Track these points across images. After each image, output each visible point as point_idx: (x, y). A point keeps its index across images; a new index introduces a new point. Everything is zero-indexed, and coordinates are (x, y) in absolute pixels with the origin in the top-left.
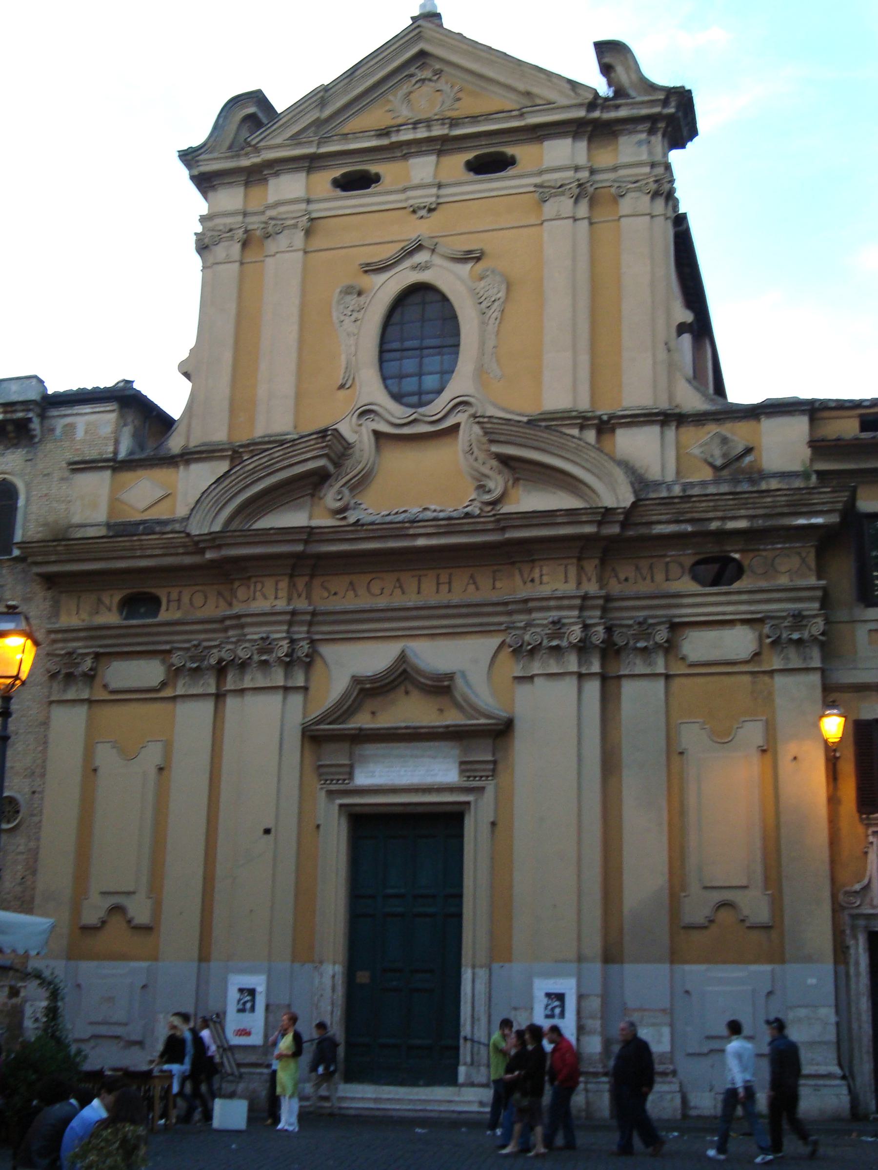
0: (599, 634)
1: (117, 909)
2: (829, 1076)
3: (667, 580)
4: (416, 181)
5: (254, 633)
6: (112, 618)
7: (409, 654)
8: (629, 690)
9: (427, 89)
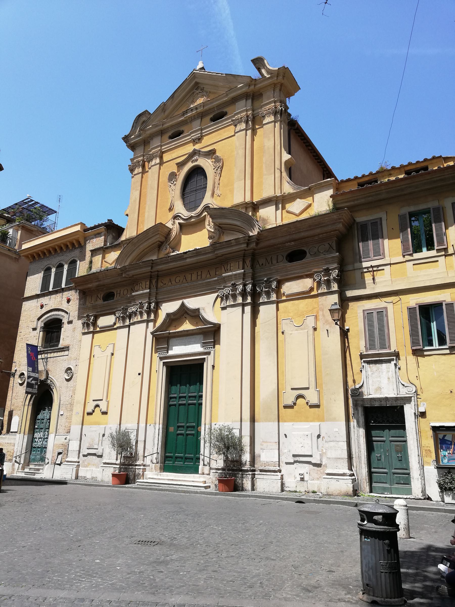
0: (249, 288)
1: (97, 406)
2: (344, 475)
6: (100, 302)
8: (262, 308)
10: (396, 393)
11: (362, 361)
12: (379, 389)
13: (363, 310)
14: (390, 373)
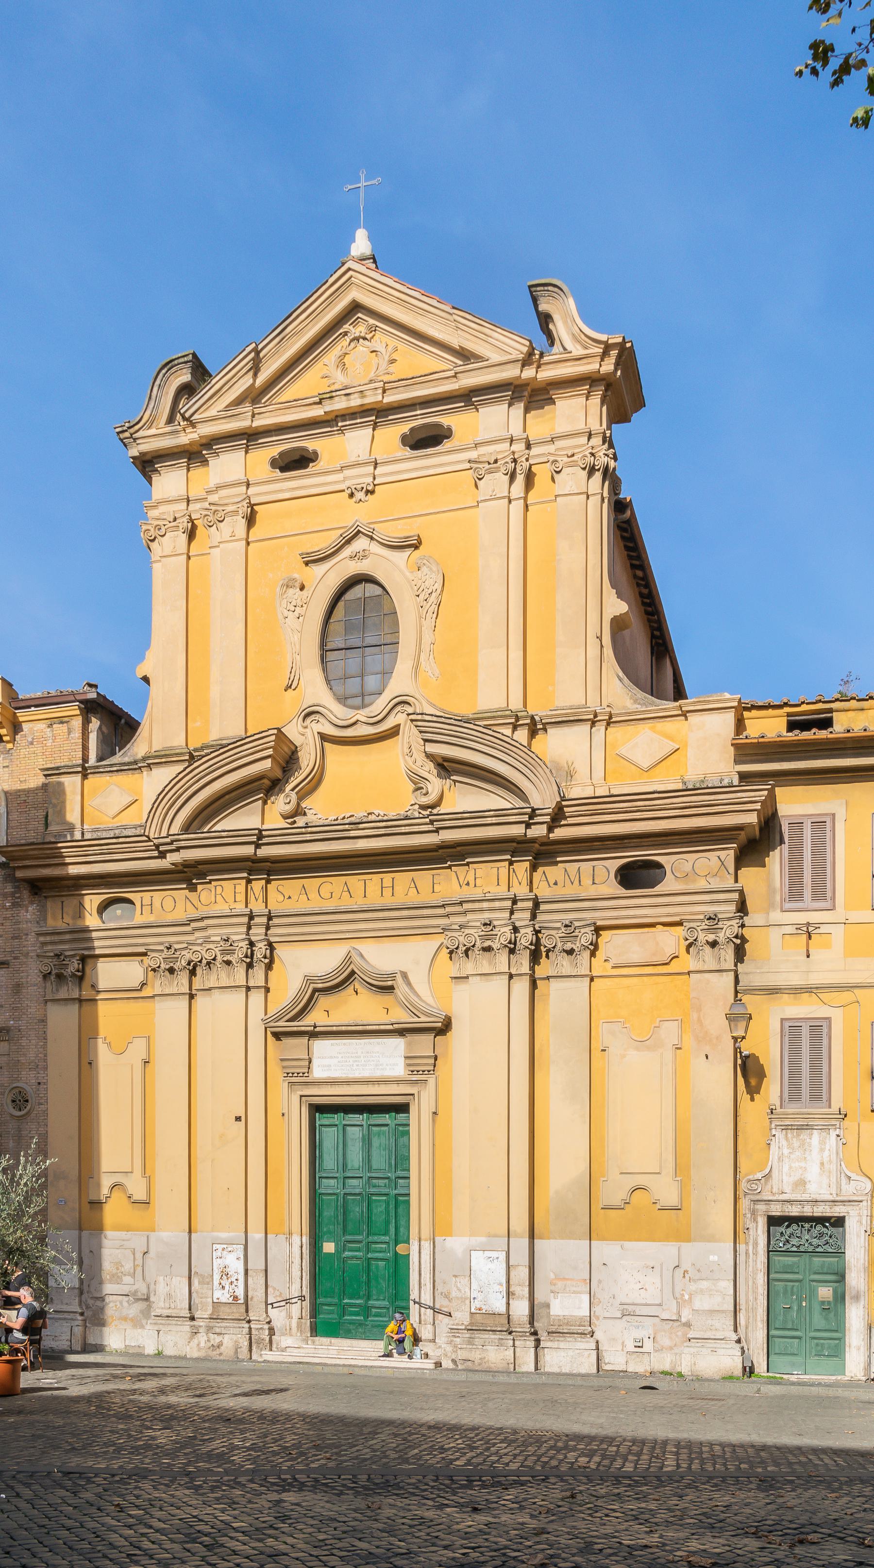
3: (594, 883)
4: (353, 459)
5: (216, 934)
7: (356, 959)
9: (362, 348)
10: (834, 1193)
11: (773, 1126)
12: (801, 1183)
13: (782, 1020)
14: (826, 1153)
